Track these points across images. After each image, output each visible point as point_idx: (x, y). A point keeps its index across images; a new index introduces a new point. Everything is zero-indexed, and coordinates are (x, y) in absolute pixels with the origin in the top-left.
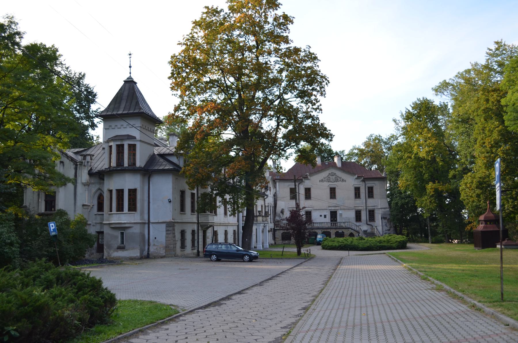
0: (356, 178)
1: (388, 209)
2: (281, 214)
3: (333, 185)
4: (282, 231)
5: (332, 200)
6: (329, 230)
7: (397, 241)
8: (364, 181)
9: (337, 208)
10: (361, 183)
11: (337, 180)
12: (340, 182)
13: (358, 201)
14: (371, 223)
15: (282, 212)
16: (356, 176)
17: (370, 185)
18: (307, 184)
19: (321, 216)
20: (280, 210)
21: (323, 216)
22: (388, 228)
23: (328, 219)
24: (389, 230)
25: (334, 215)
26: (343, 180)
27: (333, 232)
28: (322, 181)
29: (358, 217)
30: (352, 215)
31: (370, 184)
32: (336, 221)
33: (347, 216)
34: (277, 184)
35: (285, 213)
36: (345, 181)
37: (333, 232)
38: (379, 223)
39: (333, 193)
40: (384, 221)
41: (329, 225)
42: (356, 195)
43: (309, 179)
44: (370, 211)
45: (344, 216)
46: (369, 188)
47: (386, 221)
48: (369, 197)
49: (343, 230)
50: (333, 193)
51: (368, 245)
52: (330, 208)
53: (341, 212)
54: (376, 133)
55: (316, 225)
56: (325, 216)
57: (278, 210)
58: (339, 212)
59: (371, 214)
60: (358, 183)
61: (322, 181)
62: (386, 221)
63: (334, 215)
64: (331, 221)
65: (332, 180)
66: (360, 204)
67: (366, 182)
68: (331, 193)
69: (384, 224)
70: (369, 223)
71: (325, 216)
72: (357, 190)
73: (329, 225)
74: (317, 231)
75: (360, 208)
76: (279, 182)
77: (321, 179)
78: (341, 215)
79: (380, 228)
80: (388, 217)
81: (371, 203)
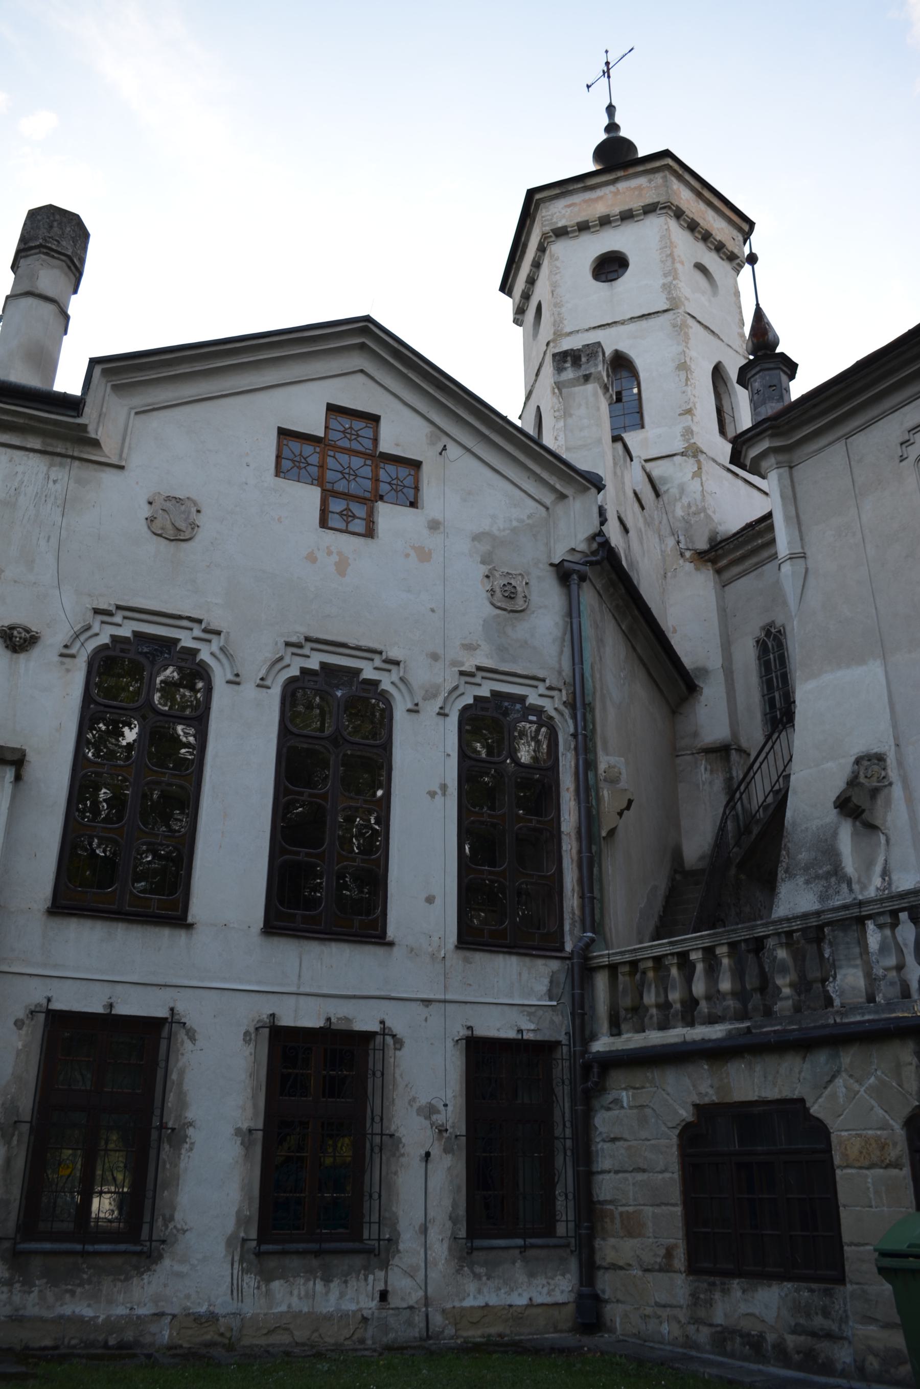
2: (846, 838)
4: (679, 1095)
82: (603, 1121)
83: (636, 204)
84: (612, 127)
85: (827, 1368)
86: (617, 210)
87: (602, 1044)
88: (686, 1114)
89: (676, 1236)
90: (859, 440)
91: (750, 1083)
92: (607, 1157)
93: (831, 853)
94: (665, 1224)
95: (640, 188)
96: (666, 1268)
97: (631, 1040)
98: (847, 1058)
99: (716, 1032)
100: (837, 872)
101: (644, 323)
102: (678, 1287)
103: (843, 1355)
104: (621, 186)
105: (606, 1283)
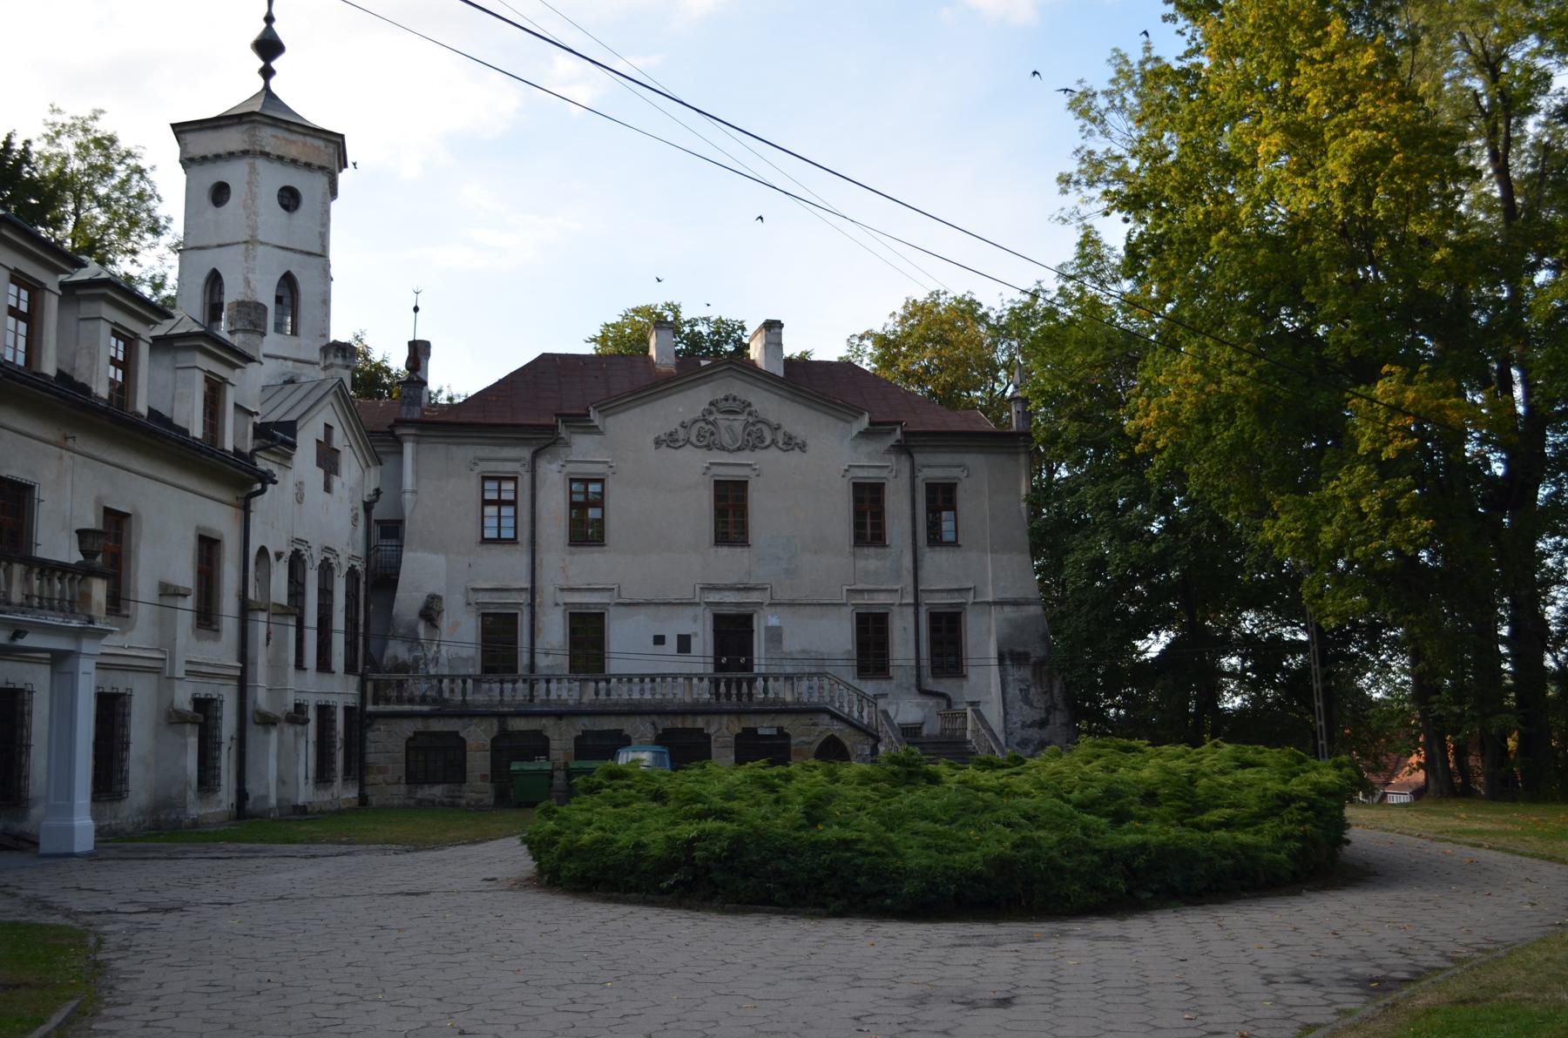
0: (864, 434)
1: (1035, 610)
2: (422, 629)
3: (732, 465)
4: (408, 728)
5: (725, 551)
6: (700, 722)
7: (1285, 800)
8: (905, 448)
9: (754, 597)
10: (892, 460)
11: (754, 442)
12: (773, 453)
13: (872, 560)
14: (944, 686)
15: (430, 612)
16: (864, 421)
17: (936, 474)
18: (584, 451)
19: (659, 640)
20: (418, 601)
21: (672, 644)
22: (1037, 715)
23: (702, 657)
24: (1042, 724)
25: (733, 633)
26: (791, 444)
27: (722, 731)
28: (669, 441)
29: (872, 633)
30: (836, 636)
31: (937, 466)
32: (749, 666)
33: (807, 639)
34: (408, 448)
35: (445, 622)
36: (803, 447)
37: (722, 731)
38: (985, 688)
39: (731, 511)
40: (1015, 673)
41: (703, 692)
42: (859, 525)
43: (594, 430)
44: (935, 618)
45: (791, 644)
46: (932, 488)
47: (1026, 673)
48: (935, 539)
49: (785, 722)
50: (731, 511)
51: (996, 842)
52: (714, 597)
53: (773, 621)
54: (956, 286)
55: (623, 694)
56: (684, 644)
57: (408, 599)
58: (765, 621)
59: (945, 631)
60: (873, 460)
61: (669, 441)
62: (1026, 673)
63: (733, 633)
64: (719, 667)
65: (726, 439)
66: (884, 575)
67: (920, 458)
68: (720, 512)
69: (1014, 691)
70: (930, 683)
71: (684, 644)
72: (868, 503)
73: (703, 692)
74: (627, 725)
75: (882, 599)
76: (418, 440)
77: (662, 428)
78: (775, 635)
79: (994, 714)
80: (1038, 652)
81: (942, 570)
82: (370, 735)
83: (316, 162)
84: (269, 19)
85: (458, 806)
86: (303, 160)
87: (370, 708)
88: (410, 734)
89: (403, 774)
90: (454, 449)
91: (437, 726)
92: (371, 748)
93: (415, 631)
94: (399, 770)
95: (318, 148)
96: (398, 783)
97: (382, 708)
98: (475, 721)
99: (426, 708)
100: (416, 639)
101: (306, 258)
102: (403, 788)
103: (463, 802)
104: (309, 140)
105: (368, 790)
